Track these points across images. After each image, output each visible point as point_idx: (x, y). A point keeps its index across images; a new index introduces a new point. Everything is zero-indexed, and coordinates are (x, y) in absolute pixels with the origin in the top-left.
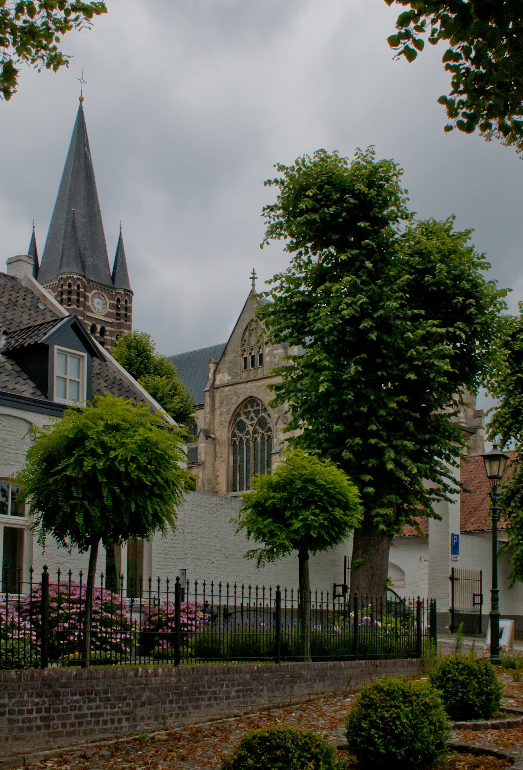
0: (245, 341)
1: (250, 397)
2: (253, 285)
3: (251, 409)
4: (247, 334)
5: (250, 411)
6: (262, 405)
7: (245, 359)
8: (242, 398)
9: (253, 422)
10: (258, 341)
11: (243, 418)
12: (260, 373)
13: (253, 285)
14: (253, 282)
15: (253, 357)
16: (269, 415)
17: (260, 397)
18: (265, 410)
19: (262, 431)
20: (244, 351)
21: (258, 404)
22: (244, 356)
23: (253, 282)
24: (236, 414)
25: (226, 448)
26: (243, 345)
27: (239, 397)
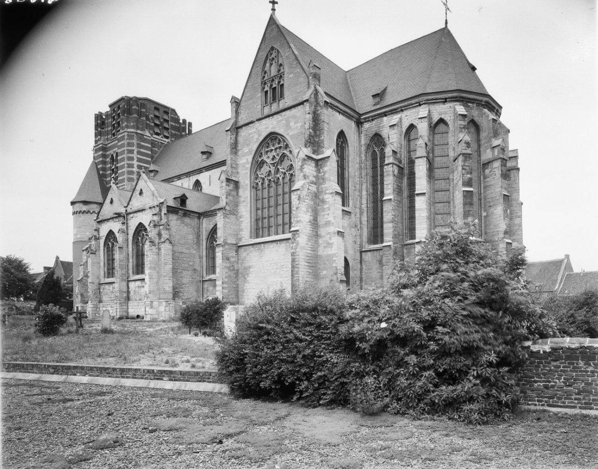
0: (265, 72)
1: (272, 133)
2: (273, 10)
3: (273, 148)
4: (268, 65)
5: (272, 150)
6: (284, 141)
7: (266, 92)
8: (264, 135)
9: (275, 161)
10: (279, 70)
11: (264, 158)
12: (283, 104)
13: (273, 10)
14: (273, 6)
15: (274, 89)
16: (291, 152)
17: (281, 131)
18: (287, 146)
19: (283, 171)
20: (265, 83)
21: (280, 140)
22: (265, 90)
23: (273, 6)
24: (258, 153)
25: (248, 192)
26: (264, 77)
27: (260, 135)
